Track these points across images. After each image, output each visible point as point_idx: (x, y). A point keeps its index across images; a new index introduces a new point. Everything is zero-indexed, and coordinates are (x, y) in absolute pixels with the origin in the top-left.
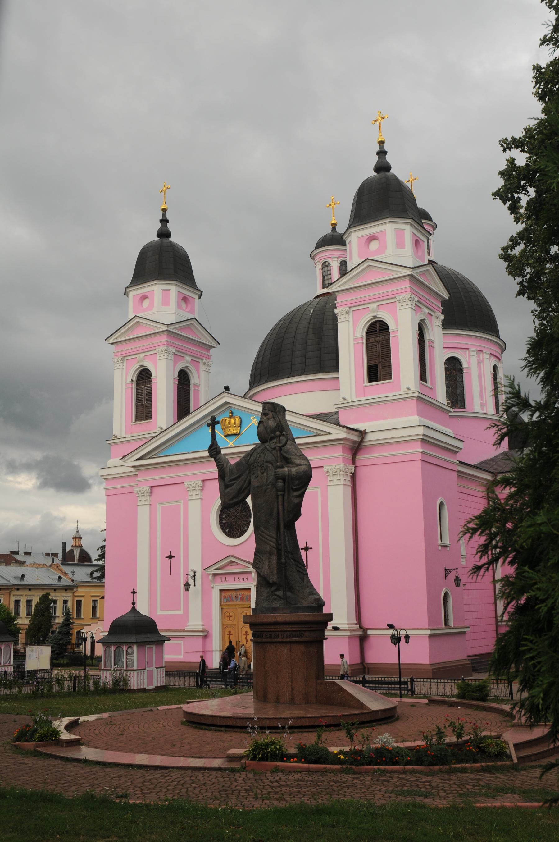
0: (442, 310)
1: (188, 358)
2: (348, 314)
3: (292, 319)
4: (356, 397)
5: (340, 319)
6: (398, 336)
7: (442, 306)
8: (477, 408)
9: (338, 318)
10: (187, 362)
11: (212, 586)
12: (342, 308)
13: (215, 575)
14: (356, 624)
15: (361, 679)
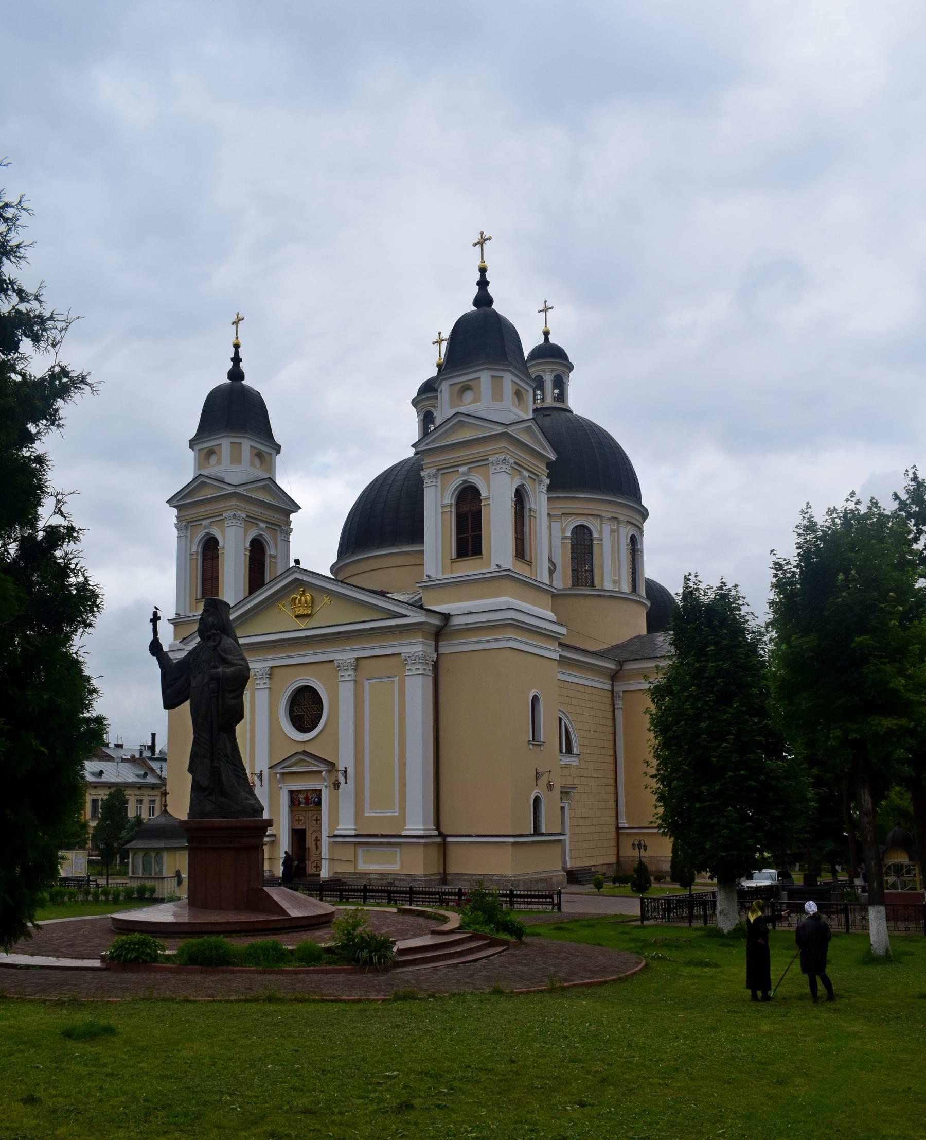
0: (548, 474)
1: (263, 525)
2: (436, 478)
3: (385, 479)
4: (443, 573)
5: (427, 483)
6: (489, 504)
7: (547, 468)
8: (608, 586)
9: (425, 482)
10: (262, 529)
11: (280, 786)
12: (428, 470)
13: (283, 774)
14: (435, 830)
15: (457, 890)
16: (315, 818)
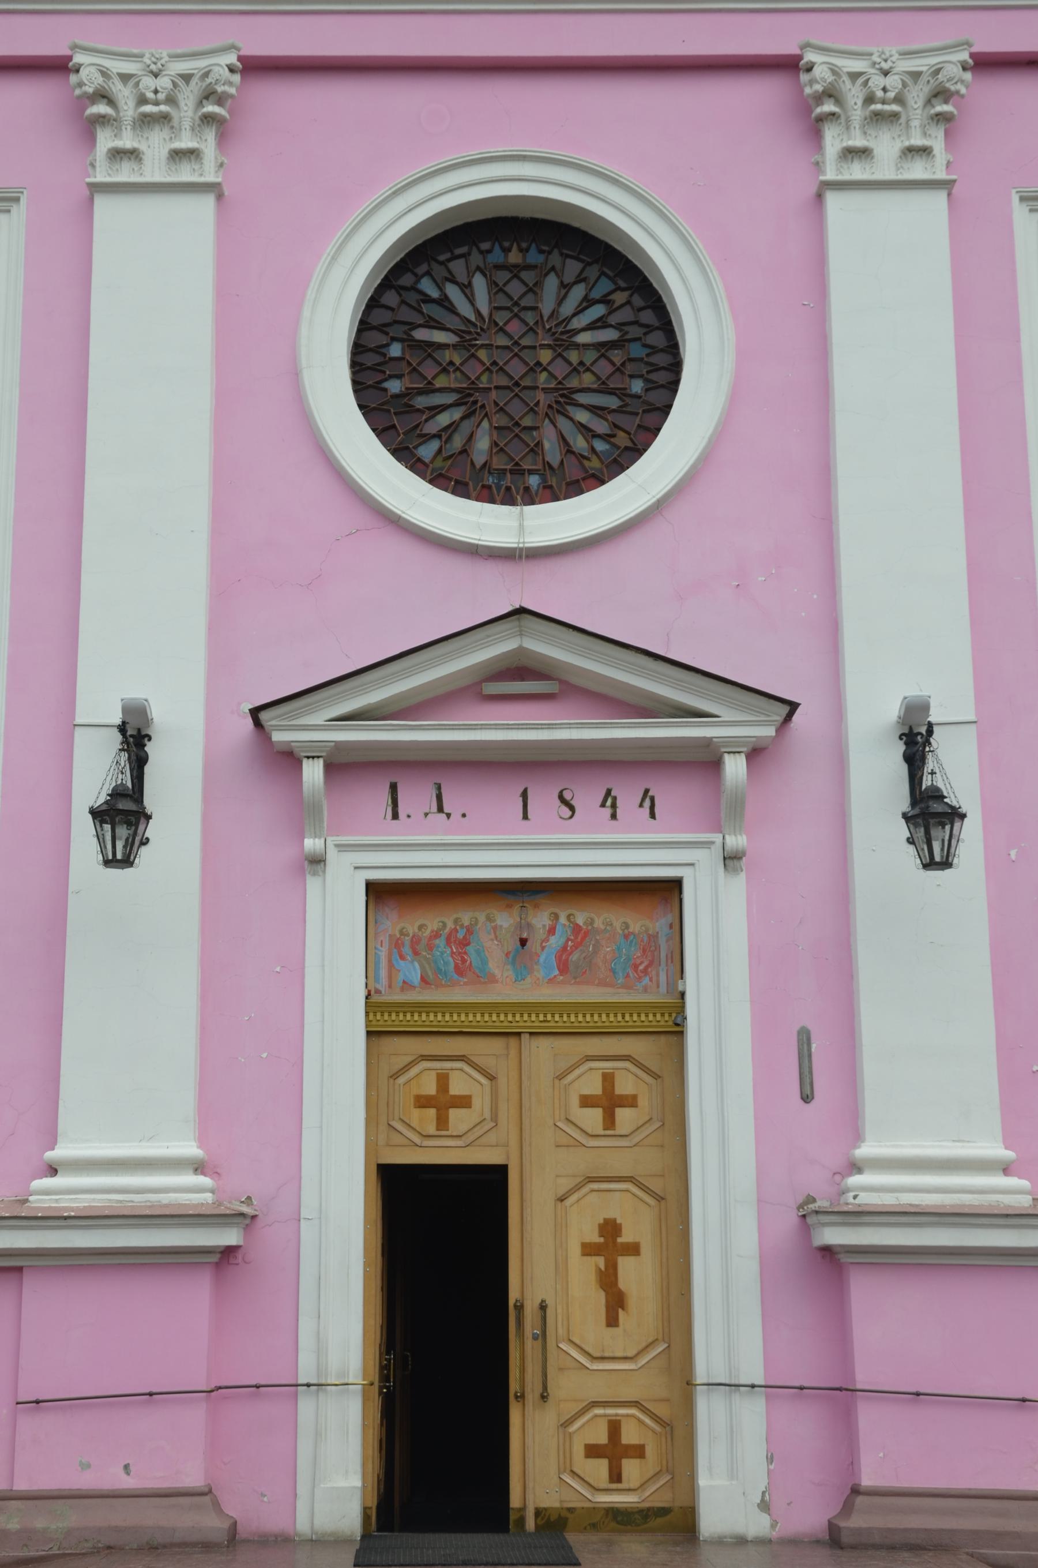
11: (311, 844)
16: (593, 1086)
